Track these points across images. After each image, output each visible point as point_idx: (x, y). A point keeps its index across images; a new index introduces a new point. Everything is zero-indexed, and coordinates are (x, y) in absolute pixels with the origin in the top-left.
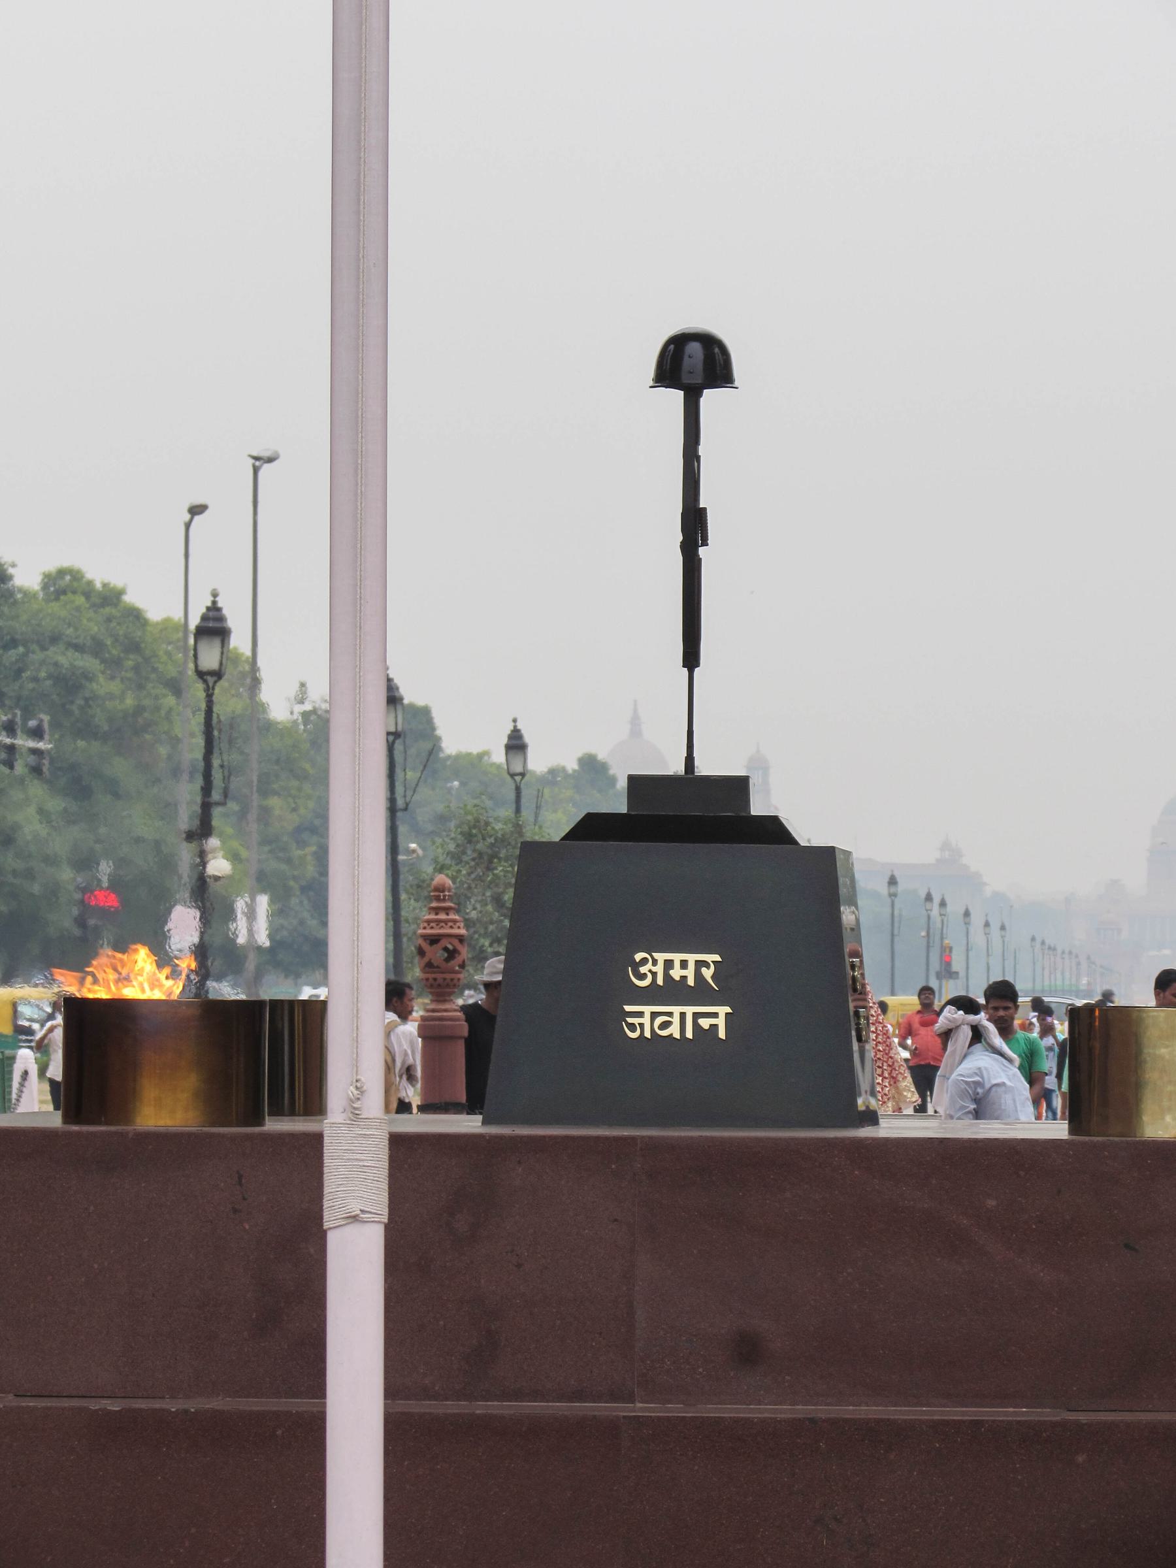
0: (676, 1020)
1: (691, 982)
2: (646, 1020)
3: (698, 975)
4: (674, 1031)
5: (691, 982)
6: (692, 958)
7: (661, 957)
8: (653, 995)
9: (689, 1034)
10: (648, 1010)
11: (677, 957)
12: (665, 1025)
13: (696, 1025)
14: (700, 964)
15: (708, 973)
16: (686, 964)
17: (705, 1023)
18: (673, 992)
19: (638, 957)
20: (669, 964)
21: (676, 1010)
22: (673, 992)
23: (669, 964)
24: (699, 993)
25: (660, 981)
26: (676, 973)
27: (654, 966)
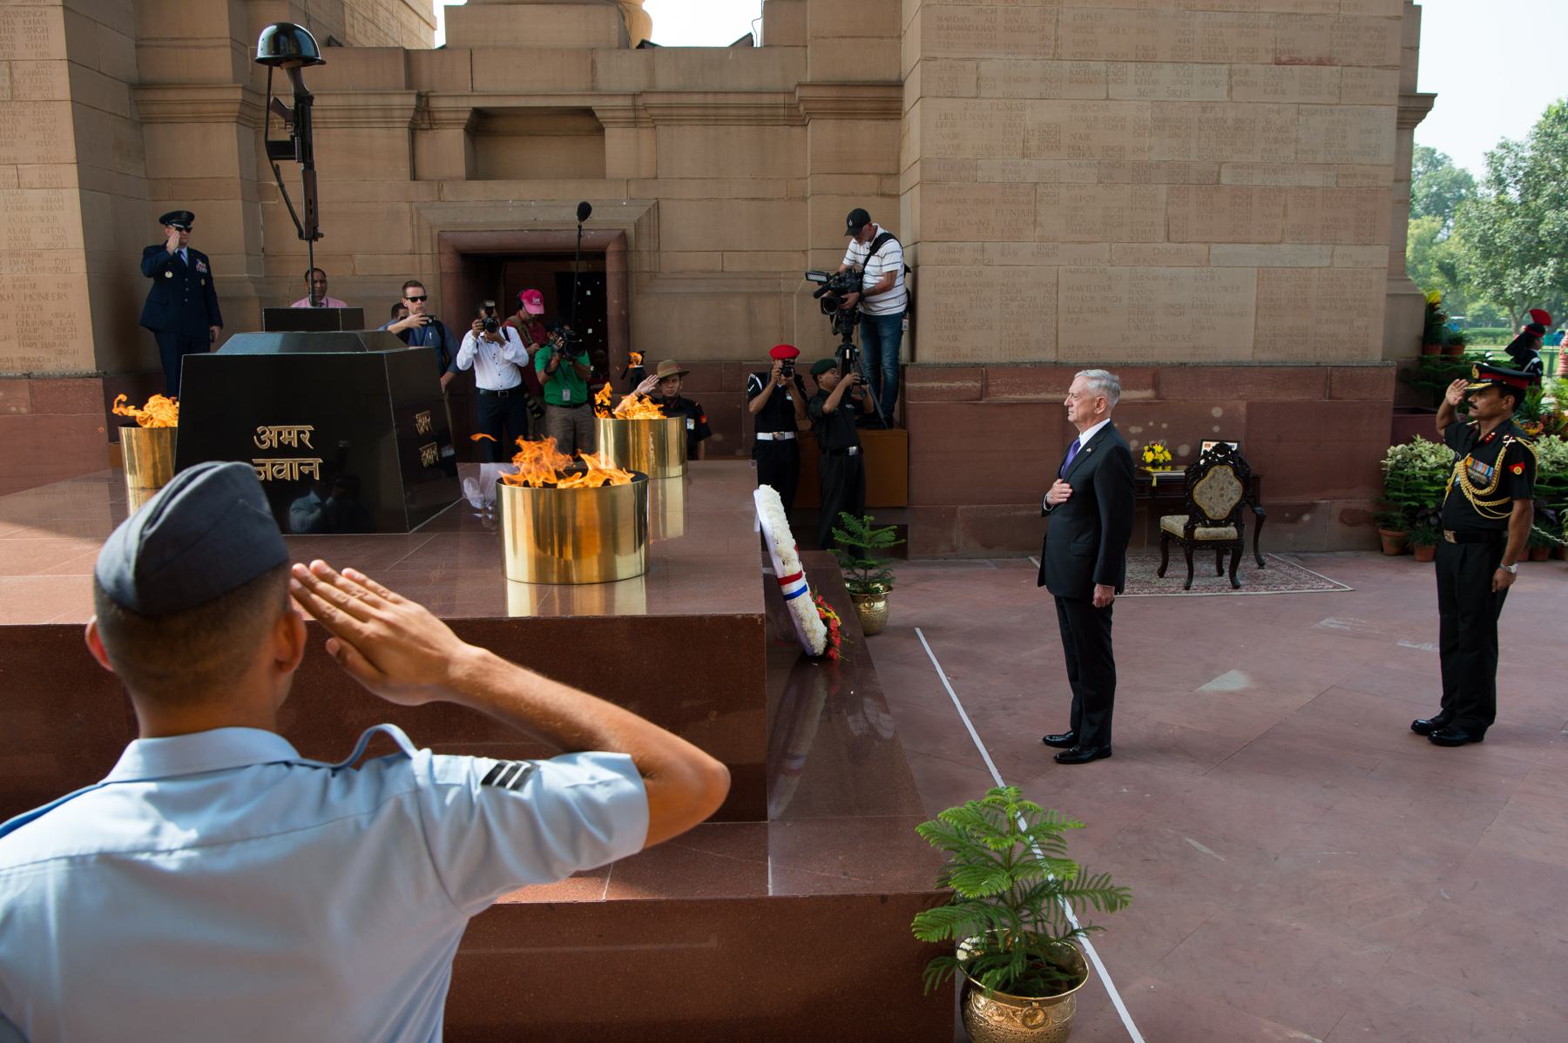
0: (286, 466)
1: (295, 444)
2: (268, 466)
3: (299, 440)
4: (286, 475)
5: (295, 444)
6: (295, 428)
7: (275, 429)
8: (271, 453)
9: (296, 477)
10: (269, 462)
11: (284, 429)
12: (280, 471)
13: (301, 473)
14: (299, 433)
15: (306, 438)
16: (290, 434)
17: (306, 470)
18: (284, 451)
19: (259, 429)
20: (280, 434)
21: (286, 462)
22: (284, 451)
23: (280, 434)
24: (301, 451)
25: (275, 445)
26: (285, 438)
27: (270, 435)
